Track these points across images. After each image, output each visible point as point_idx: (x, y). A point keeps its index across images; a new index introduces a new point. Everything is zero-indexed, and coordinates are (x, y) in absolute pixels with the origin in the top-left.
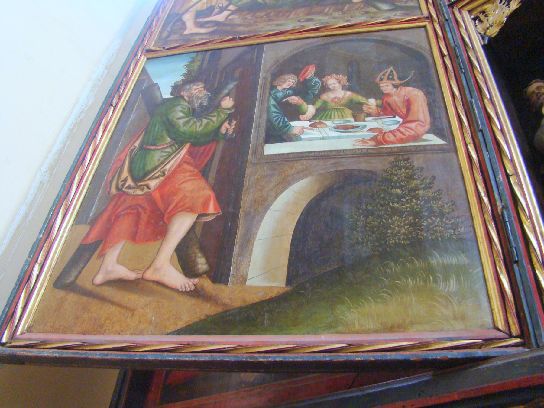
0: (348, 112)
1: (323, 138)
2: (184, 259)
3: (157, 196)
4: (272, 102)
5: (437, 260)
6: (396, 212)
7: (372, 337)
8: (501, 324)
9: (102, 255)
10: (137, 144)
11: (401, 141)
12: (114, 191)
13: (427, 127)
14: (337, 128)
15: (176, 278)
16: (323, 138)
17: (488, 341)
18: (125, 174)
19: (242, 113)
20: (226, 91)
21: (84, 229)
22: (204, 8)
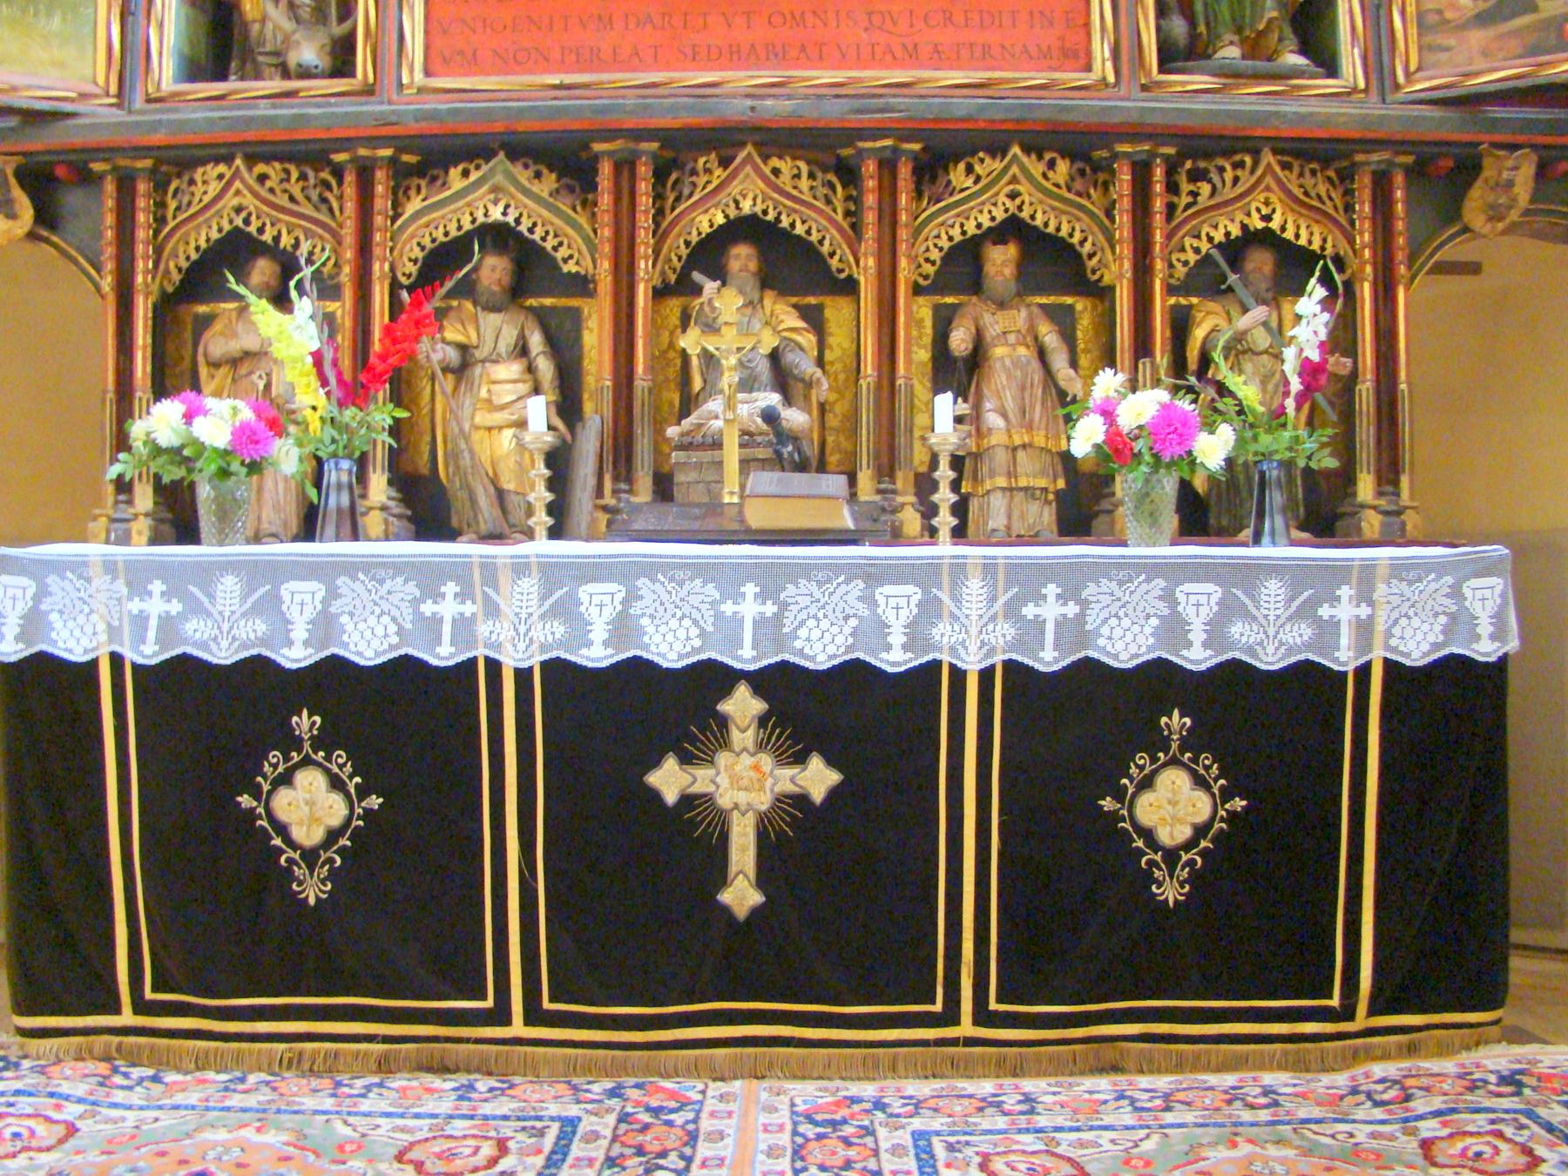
8: (101, 80)
17: (84, 96)
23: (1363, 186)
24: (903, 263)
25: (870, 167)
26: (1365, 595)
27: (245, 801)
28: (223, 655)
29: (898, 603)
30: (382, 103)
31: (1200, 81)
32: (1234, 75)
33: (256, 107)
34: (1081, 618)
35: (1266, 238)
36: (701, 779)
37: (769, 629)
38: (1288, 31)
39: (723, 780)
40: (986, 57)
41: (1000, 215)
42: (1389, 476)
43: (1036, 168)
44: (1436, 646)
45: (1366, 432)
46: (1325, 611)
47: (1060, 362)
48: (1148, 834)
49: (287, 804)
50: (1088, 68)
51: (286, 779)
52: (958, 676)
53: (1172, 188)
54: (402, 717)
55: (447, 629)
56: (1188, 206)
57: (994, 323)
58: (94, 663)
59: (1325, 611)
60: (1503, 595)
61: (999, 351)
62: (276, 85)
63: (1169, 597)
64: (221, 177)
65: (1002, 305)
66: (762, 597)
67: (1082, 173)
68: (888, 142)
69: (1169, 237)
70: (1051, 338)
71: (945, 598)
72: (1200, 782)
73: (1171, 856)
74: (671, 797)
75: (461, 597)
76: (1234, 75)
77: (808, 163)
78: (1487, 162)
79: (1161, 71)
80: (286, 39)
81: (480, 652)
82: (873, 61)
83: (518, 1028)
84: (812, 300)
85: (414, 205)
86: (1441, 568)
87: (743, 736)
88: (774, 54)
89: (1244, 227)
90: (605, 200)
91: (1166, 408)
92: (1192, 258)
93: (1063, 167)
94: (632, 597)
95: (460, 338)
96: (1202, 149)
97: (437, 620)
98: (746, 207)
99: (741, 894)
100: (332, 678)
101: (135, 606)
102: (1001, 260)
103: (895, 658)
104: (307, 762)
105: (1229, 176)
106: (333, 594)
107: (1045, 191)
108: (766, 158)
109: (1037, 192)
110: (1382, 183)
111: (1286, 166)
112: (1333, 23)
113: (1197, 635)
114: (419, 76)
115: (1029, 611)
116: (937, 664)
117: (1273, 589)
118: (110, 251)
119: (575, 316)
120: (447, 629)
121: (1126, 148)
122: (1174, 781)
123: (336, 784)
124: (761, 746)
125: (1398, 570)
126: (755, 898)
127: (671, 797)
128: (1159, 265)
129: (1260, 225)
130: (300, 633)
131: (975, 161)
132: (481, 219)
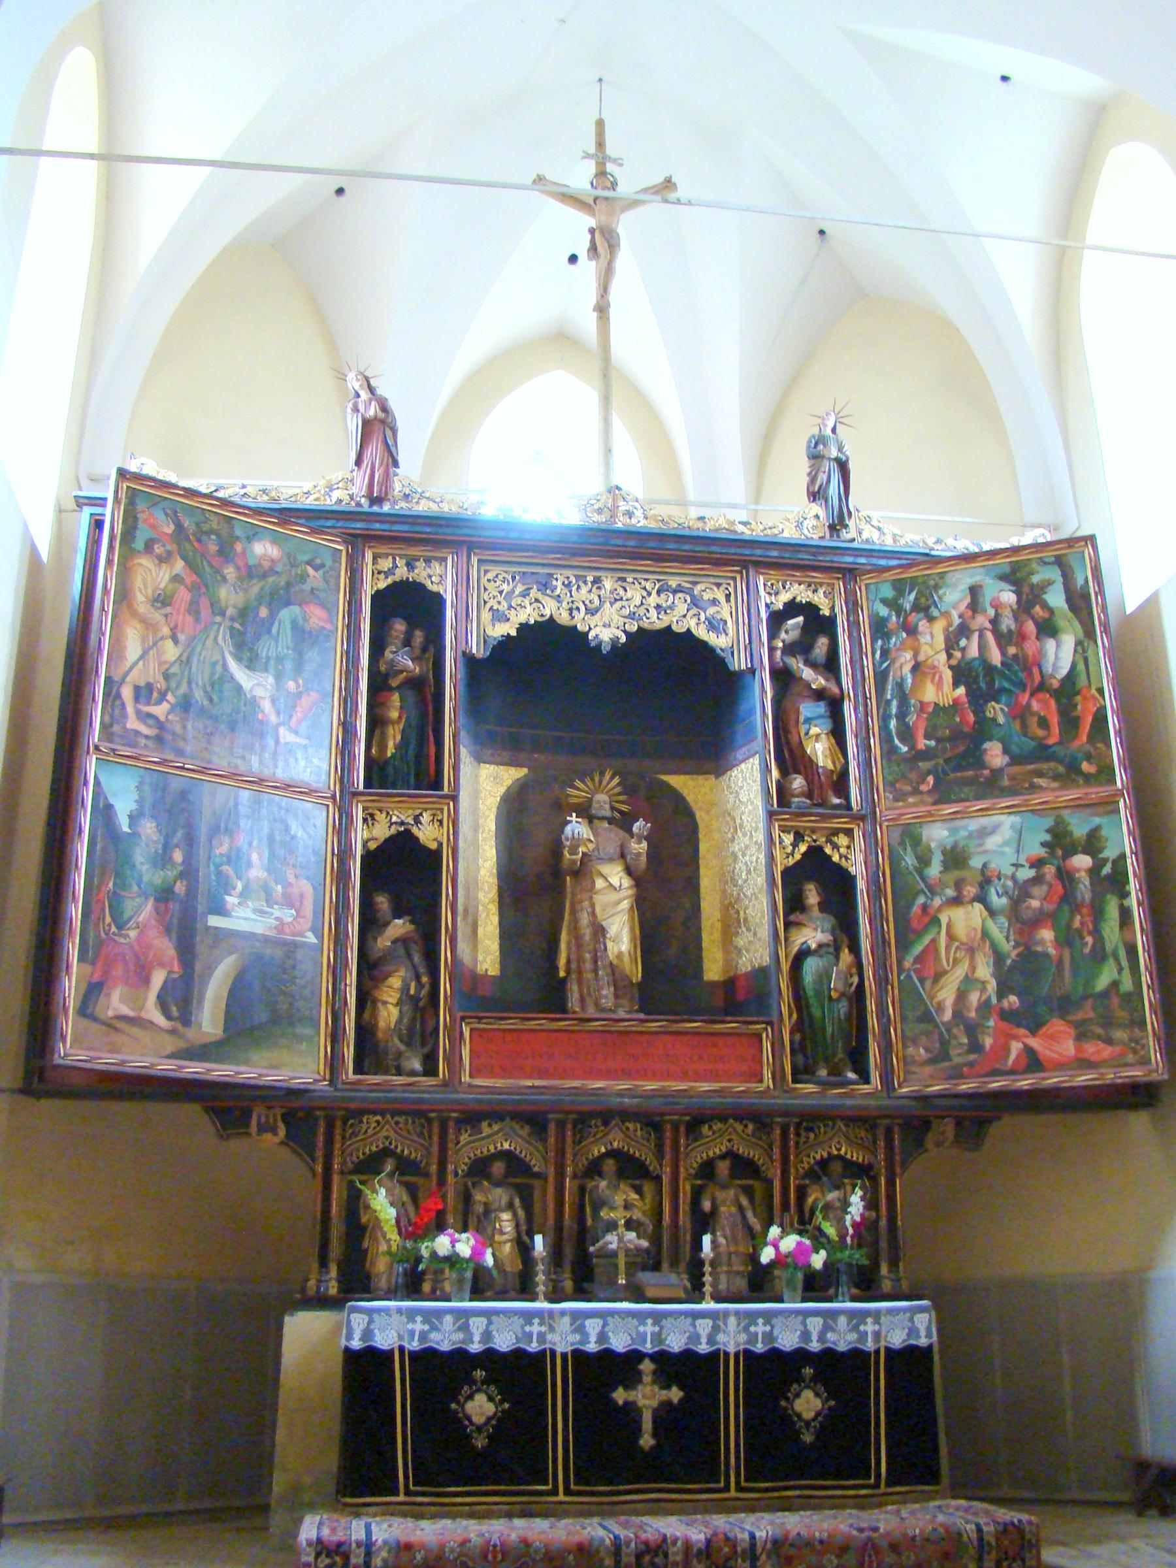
0: (263, 894)
1: (246, 919)
2: (163, 1003)
3: (137, 948)
4: (212, 868)
5: (299, 1030)
6: (282, 992)
7: (265, 1072)
9: (108, 995)
10: (111, 885)
11: (293, 935)
12: (102, 933)
13: (309, 925)
14: (255, 911)
15: (160, 1019)
16: (246, 919)
17: (316, 1081)
18: (108, 919)
20: (175, 841)
21: (88, 968)
22: (142, 684)
23: (880, 1133)
24: (682, 1169)
25: (669, 1126)
26: (877, 1321)
27: (453, 1406)
28: (445, 1347)
29: (704, 1327)
30: (452, 1093)
31: (810, 1088)
33: (396, 1091)
34: (772, 1331)
35: (841, 1158)
36: (632, 1395)
37: (658, 1337)
38: (848, 1061)
39: (640, 1396)
40: (716, 1078)
41: (724, 1149)
42: (894, 1264)
43: (739, 1127)
44: (904, 1341)
45: (884, 1244)
46: (862, 1328)
47: (750, 1215)
48: (799, 1416)
49: (470, 1407)
50: (761, 1081)
51: (470, 1397)
52: (727, 1354)
53: (798, 1135)
54: (517, 1372)
55: (535, 1337)
56: (805, 1143)
57: (720, 1195)
58: (392, 1350)
59: (862, 1328)
60: (930, 1321)
61: (723, 1209)
62: (401, 1080)
63: (804, 1324)
64: (378, 1122)
65: (724, 1187)
66: (654, 1324)
67: (759, 1129)
68: (676, 1117)
69: (796, 1156)
70: (744, 1201)
71: (721, 1324)
72: (817, 1395)
73: (807, 1424)
74: (621, 1402)
75: (540, 1324)
77: (640, 1122)
78: (934, 1127)
79: (795, 1081)
80: (399, 1055)
81: (548, 1346)
82: (668, 1076)
83: (562, 1497)
84: (637, 1182)
85: (464, 1138)
86: (904, 1310)
87: (647, 1379)
88: (627, 1074)
89: (829, 1154)
90: (552, 1140)
91: (799, 1244)
92: (806, 1166)
93: (751, 1127)
94: (605, 1325)
95: (484, 1199)
96: (811, 1120)
97: (530, 1335)
98: (615, 1144)
99: (647, 1441)
100: (490, 1357)
101: (410, 1326)
102: (723, 1167)
103: (703, 1348)
104: (478, 1390)
105: (822, 1130)
106: (490, 1323)
107: (743, 1139)
108: (623, 1122)
110: (889, 1131)
111: (847, 1126)
112: (868, 1062)
113: (814, 1337)
114: (468, 1078)
115: (752, 1329)
116: (718, 1351)
117: (842, 1320)
118: (319, 1154)
119: (530, 1187)
120: (535, 1337)
121: (778, 1120)
122: (808, 1394)
123: (491, 1399)
124: (654, 1382)
125: (890, 1311)
126: (652, 1442)
127: (621, 1402)
128: (792, 1170)
129: (836, 1153)
130: (477, 1338)
131: (712, 1124)
132: (499, 1148)
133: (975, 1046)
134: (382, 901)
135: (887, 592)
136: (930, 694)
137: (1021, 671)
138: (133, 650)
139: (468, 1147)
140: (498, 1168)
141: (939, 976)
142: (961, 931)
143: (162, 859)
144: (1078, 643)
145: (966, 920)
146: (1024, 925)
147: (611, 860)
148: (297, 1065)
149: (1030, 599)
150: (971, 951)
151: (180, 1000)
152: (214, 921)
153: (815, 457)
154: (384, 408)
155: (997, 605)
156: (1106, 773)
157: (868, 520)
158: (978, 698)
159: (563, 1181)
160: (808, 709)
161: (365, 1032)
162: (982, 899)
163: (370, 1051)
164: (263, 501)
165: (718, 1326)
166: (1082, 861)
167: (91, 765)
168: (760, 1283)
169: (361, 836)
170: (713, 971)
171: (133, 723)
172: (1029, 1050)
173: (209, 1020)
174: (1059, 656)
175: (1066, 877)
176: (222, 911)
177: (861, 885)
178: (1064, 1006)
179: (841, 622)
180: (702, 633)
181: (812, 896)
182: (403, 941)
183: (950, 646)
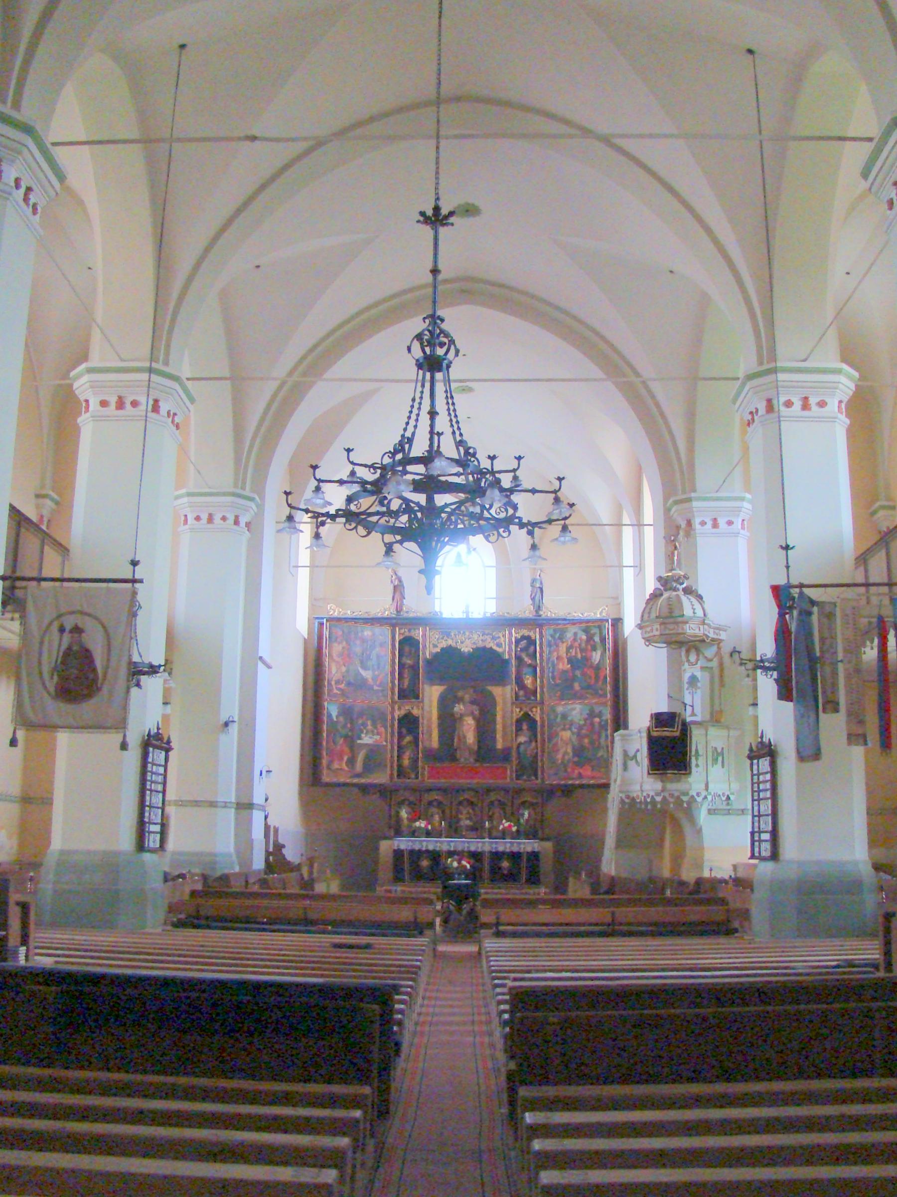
2: (347, 765)
15: (346, 768)
19: (352, 730)
29: (480, 845)
32: (525, 781)
76: (525, 781)
96: (519, 791)
100: (427, 851)
103: (480, 850)
109: (500, 796)
133: (566, 771)
134: (404, 731)
135: (551, 632)
136: (561, 666)
137: (587, 659)
138: (334, 670)
139: (427, 797)
140: (435, 803)
141: (558, 751)
142: (564, 738)
143: (345, 726)
144: (602, 654)
145: (566, 734)
146: (580, 736)
147: (468, 715)
148: (381, 778)
149: (590, 638)
150: (567, 744)
151: (351, 762)
152: (359, 742)
153: (532, 586)
154: (400, 581)
155: (581, 639)
156: (605, 696)
157: (547, 608)
158: (574, 668)
159: (457, 805)
160: (526, 670)
161: (400, 766)
162: (570, 729)
163: (401, 773)
164: (366, 616)
165: (485, 845)
166: (597, 720)
167: (326, 704)
168: (504, 835)
169: (397, 714)
170: (500, 745)
171: (335, 691)
172: (580, 774)
173: (359, 767)
174: (596, 657)
175: (592, 724)
176: (360, 738)
177: (539, 723)
178: (589, 760)
179: (538, 642)
180: (495, 648)
181: (525, 727)
182: (410, 742)
183: (567, 651)
